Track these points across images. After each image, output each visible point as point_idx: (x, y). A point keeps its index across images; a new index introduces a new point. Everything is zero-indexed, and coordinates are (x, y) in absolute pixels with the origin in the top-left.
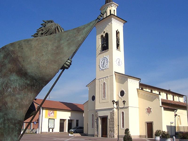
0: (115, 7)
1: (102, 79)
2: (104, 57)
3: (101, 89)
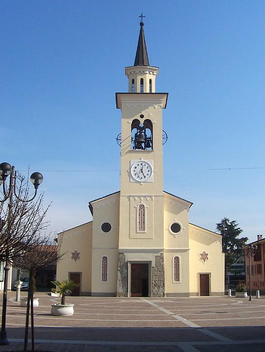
0: (142, 72)
1: (136, 198)
2: (142, 160)
3: (133, 215)
